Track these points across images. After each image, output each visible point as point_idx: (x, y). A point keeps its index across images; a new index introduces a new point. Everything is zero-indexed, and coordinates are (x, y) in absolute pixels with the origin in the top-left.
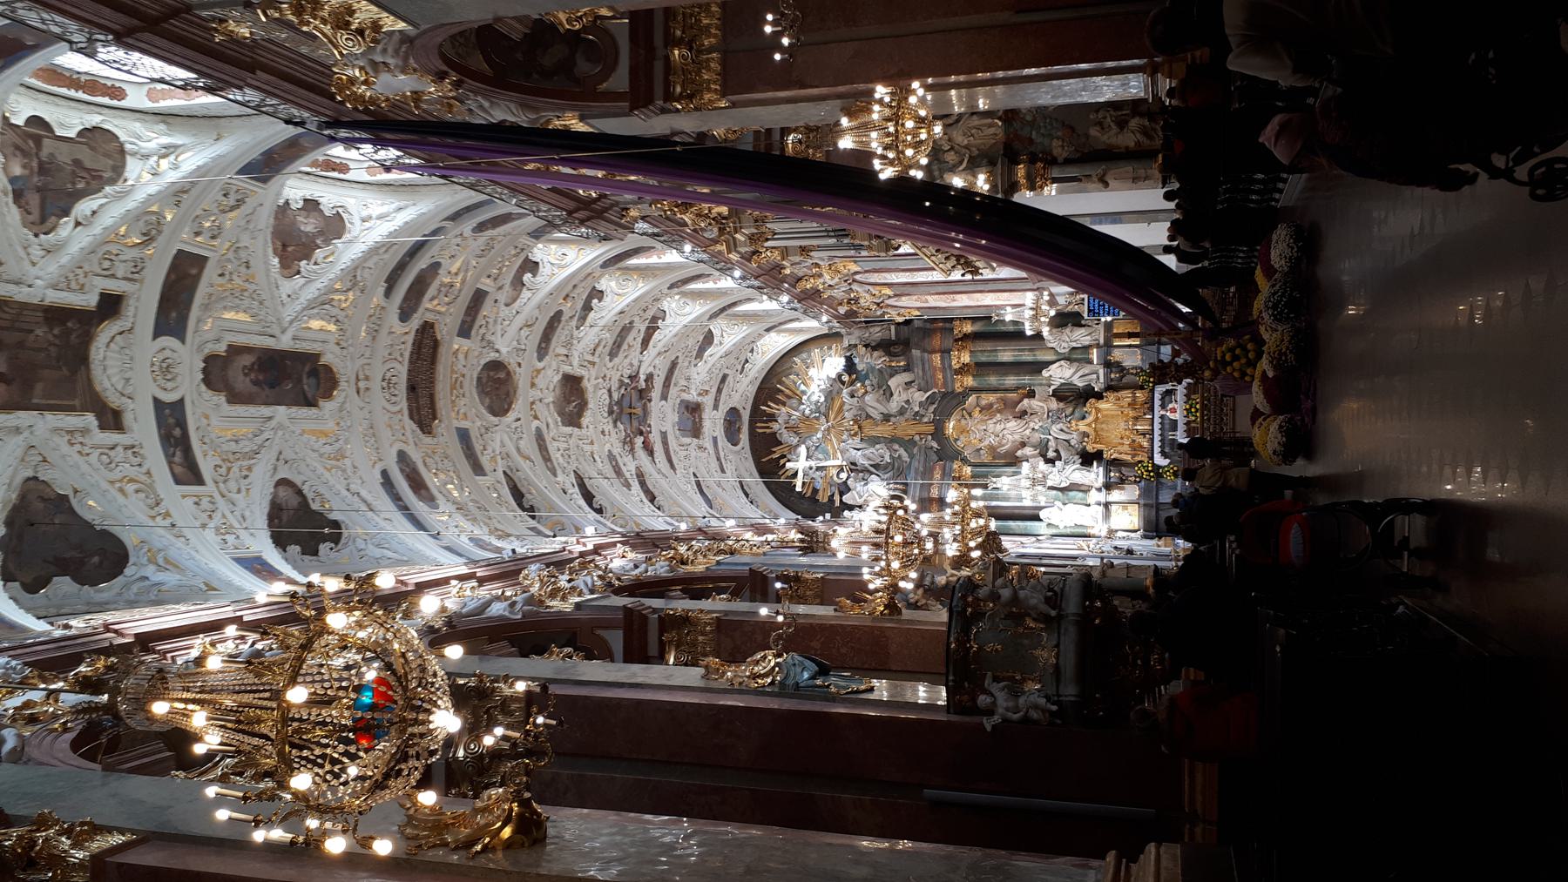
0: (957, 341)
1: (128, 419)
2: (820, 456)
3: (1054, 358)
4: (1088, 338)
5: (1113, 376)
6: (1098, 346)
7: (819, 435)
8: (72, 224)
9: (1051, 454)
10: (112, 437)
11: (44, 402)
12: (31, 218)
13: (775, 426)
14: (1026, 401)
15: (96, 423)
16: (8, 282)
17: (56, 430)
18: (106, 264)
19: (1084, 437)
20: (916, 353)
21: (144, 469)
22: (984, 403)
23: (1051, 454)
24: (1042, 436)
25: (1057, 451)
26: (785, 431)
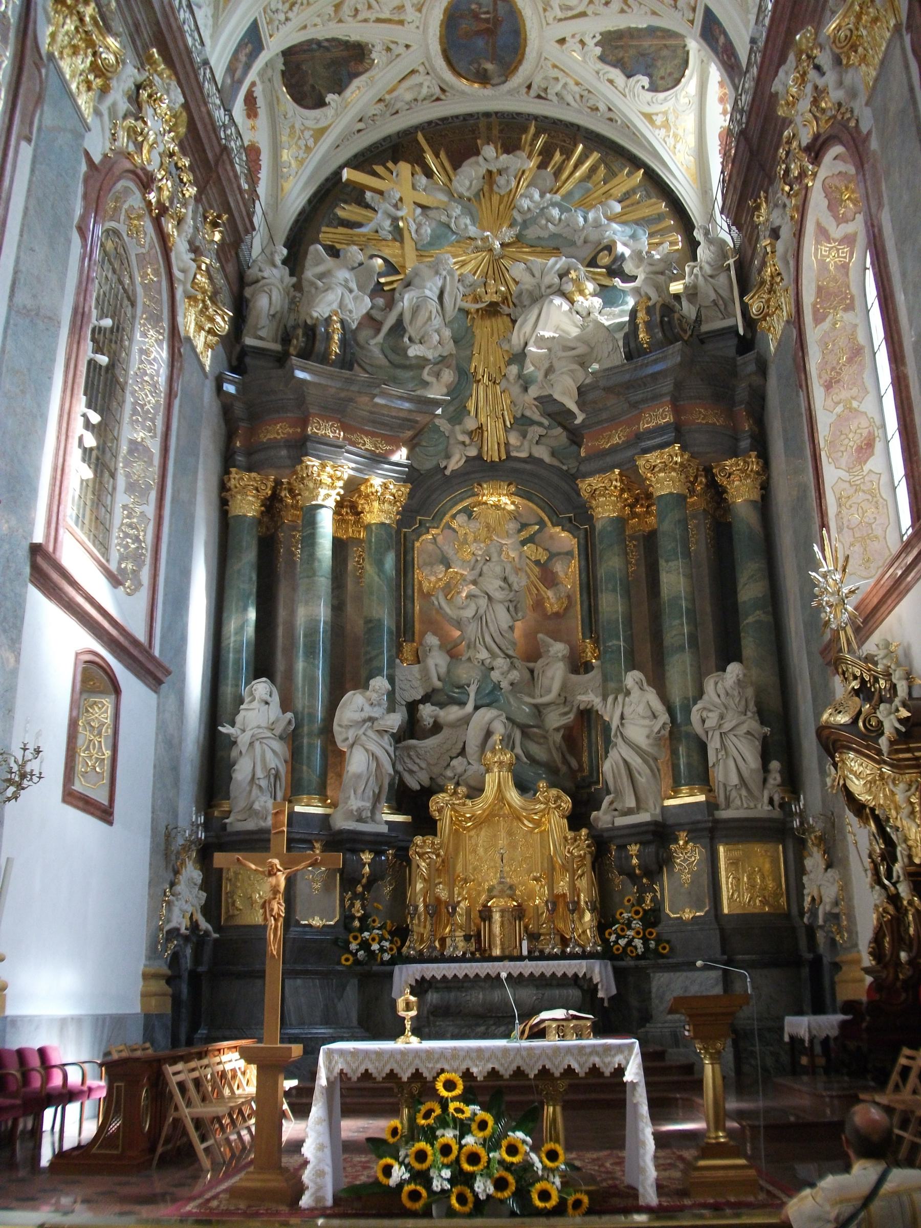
0: (708, 471)
2: (427, 230)
3: (677, 700)
4: (734, 780)
5: (634, 849)
6: (711, 806)
7: (473, 231)
9: (427, 712)
13: (489, 151)
14: (559, 648)
19: (469, 787)
20: (673, 355)
22: (558, 568)
23: (427, 712)
24: (472, 690)
25: (437, 728)
26: (482, 171)
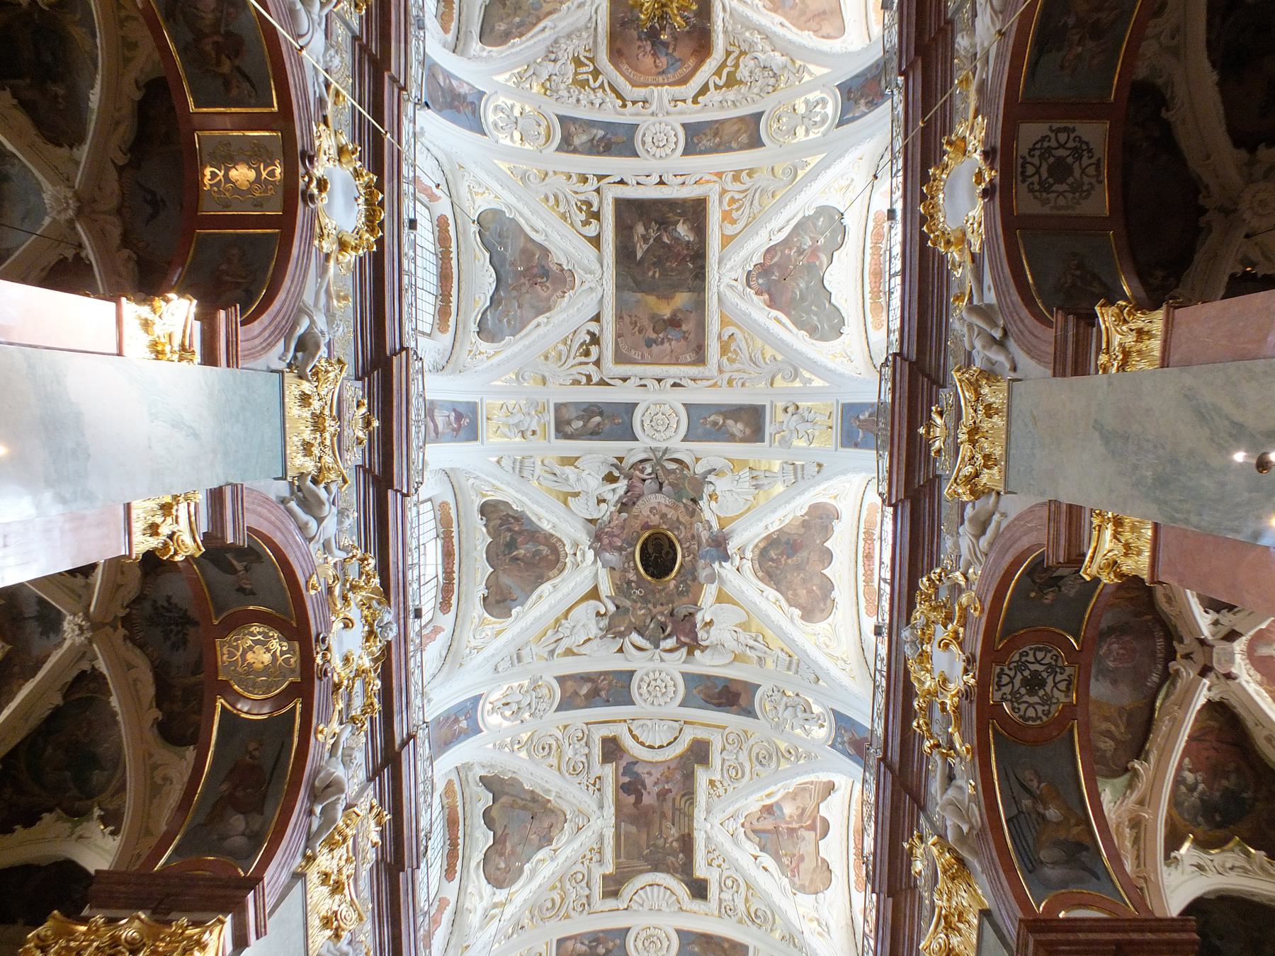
1: (611, 903)
8: (756, 854)
10: (597, 889)
11: (622, 833)
12: (755, 822)
15: (607, 872)
16: (707, 803)
17: (601, 838)
18: (729, 883)
21: (572, 913)
